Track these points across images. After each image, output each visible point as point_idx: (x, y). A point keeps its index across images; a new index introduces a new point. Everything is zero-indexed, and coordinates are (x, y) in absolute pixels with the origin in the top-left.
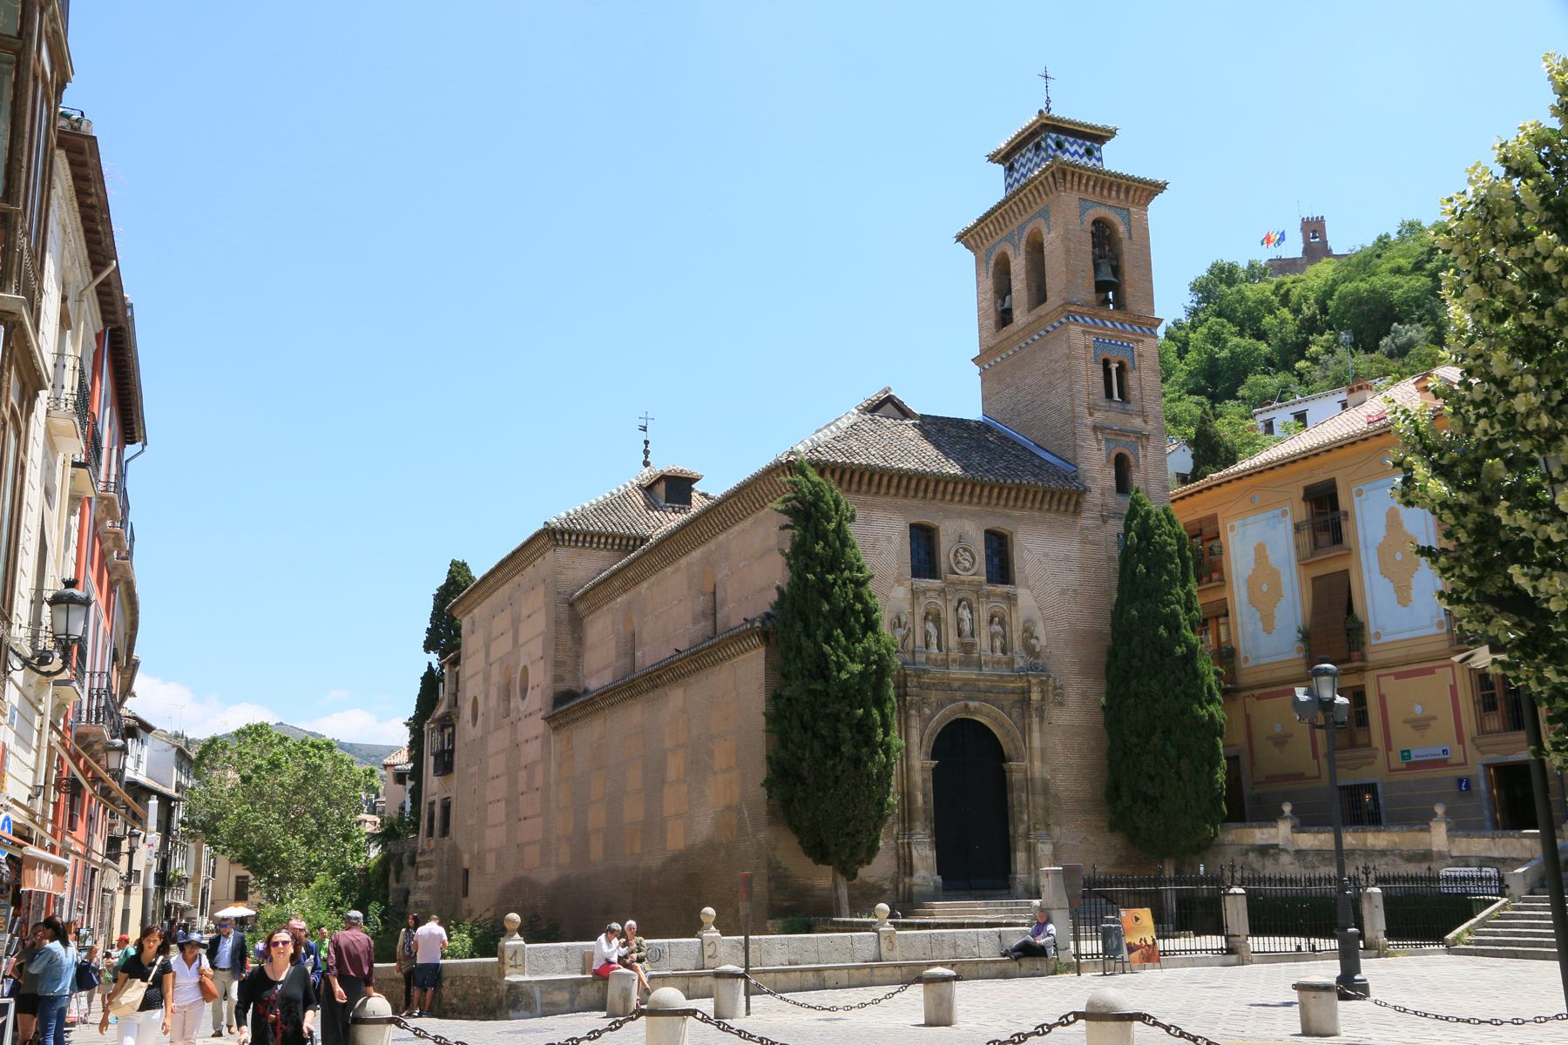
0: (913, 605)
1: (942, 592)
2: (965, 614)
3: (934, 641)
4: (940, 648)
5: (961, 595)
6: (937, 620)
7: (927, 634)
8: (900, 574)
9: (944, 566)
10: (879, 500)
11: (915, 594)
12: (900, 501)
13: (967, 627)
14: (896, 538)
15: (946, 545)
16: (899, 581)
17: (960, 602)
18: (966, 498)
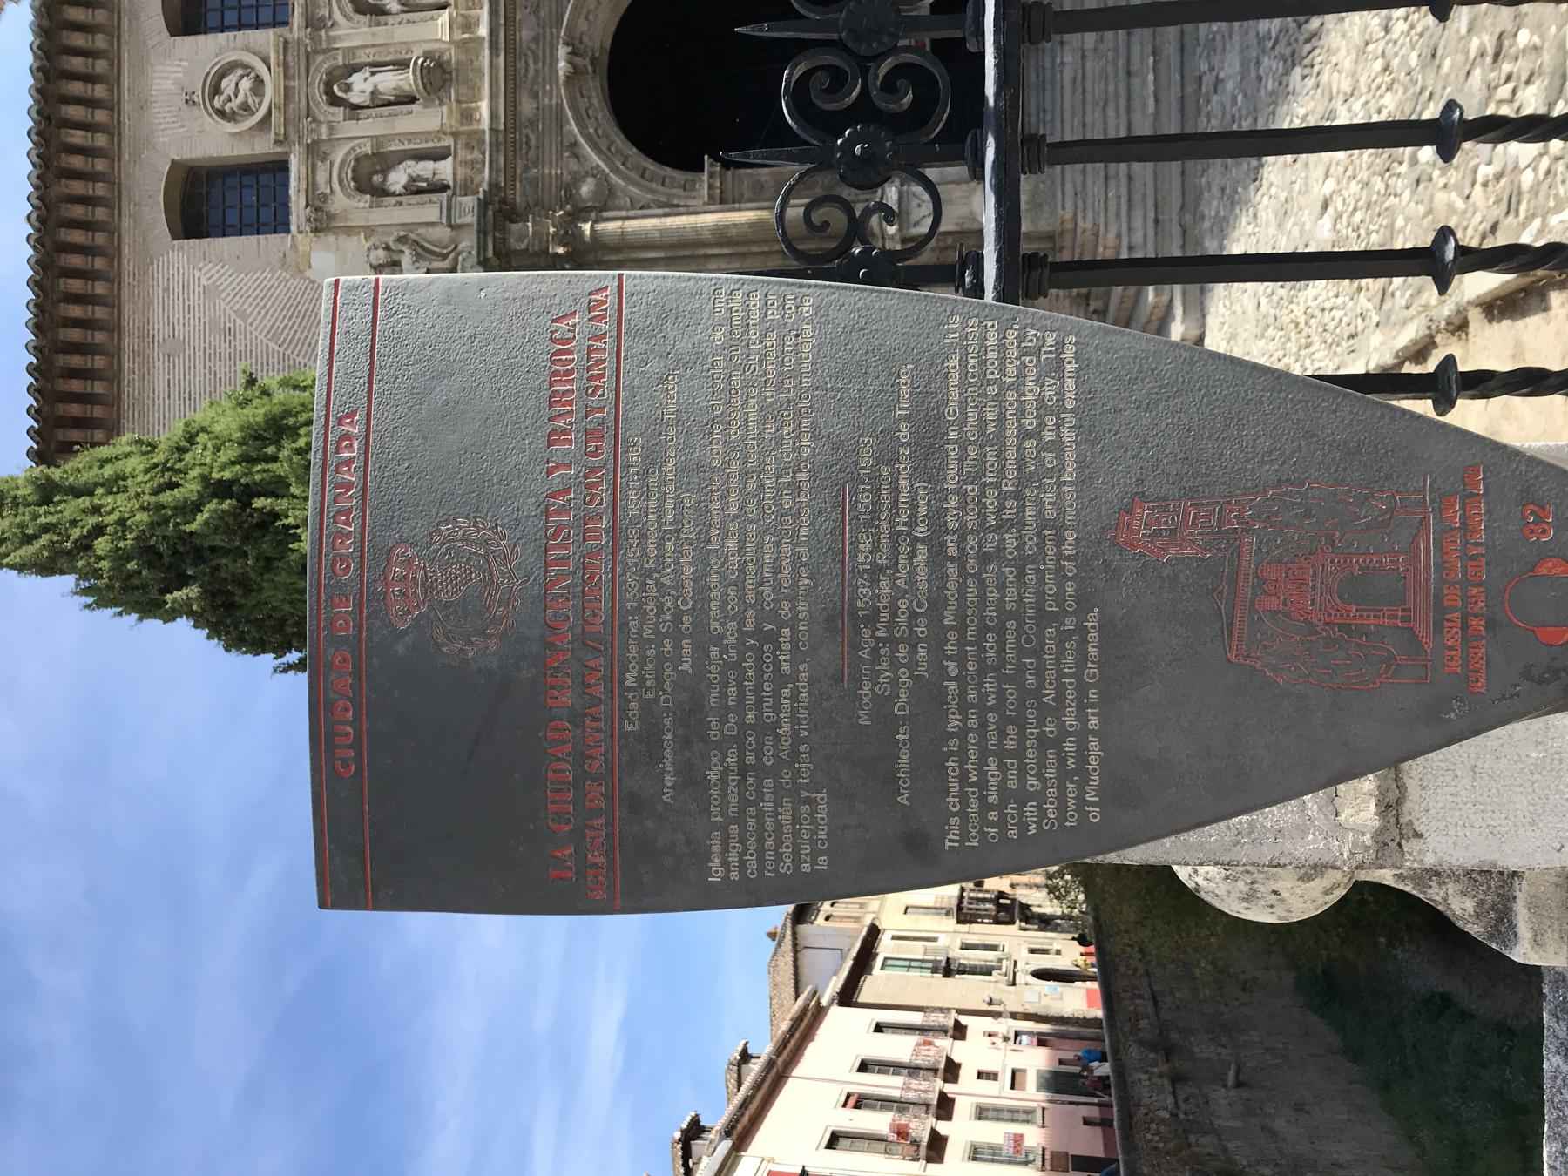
0: (350, 231)
1: (315, 152)
2: (361, 86)
3: (425, 168)
4: (438, 156)
5: (318, 91)
6: (383, 160)
7: (415, 189)
8: (284, 264)
9: (263, 147)
10: (130, 321)
11: (322, 222)
12: (128, 266)
13: (389, 82)
14: (208, 274)
15: (216, 141)
16: (300, 268)
17: (335, 101)
18: (100, 91)
